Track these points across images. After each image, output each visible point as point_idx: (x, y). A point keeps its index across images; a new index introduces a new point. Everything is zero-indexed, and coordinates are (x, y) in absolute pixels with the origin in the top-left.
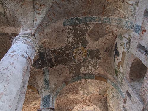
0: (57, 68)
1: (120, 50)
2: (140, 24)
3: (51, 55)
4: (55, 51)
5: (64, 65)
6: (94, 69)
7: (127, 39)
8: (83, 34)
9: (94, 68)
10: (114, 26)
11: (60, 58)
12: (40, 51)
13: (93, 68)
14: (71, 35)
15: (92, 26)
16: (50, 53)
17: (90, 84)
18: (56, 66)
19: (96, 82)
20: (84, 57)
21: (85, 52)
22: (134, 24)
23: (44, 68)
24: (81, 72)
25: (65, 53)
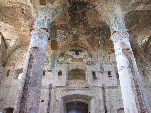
0: (67, 15)
1: (82, 55)
2: (104, 70)
3: (81, 11)
4: (84, 14)
5: (70, 20)
6: (61, 39)
7: (92, 61)
8: (93, 33)
9: (63, 39)
10: (98, 52)
11: (76, 17)
12: (89, 5)
14: (95, 27)
15: (98, 38)
16: (83, 11)
18: (69, 14)
20: (74, 33)
21: (78, 34)
22: (103, 66)
23: (68, 5)
24: (58, 31)
25: (80, 21)
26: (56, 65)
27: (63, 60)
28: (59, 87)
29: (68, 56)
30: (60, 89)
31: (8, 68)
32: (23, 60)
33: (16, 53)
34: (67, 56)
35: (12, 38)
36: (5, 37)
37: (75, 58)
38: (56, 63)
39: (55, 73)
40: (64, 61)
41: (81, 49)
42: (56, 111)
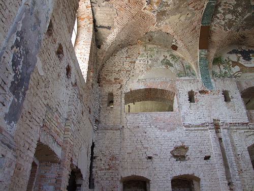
6: (223, 23)
9: (226, 23)
13: (226, 21)
17: (189, 16)
19: (192, 27)
26: (212, 80)
27: (224, 71)
28: (235, 124)
29: (231, 63)
30: (239, 129)
31: (107, 89)
32: (137, 71)
33: (117, 59)
34: (228, 63)
35: (116, 24)
36: (99, 23)
37: (246, 65)
38: (211, 76)
39: (216, 96)
40: (226, 73)
41: (250, 49)
42: (246, 180)
